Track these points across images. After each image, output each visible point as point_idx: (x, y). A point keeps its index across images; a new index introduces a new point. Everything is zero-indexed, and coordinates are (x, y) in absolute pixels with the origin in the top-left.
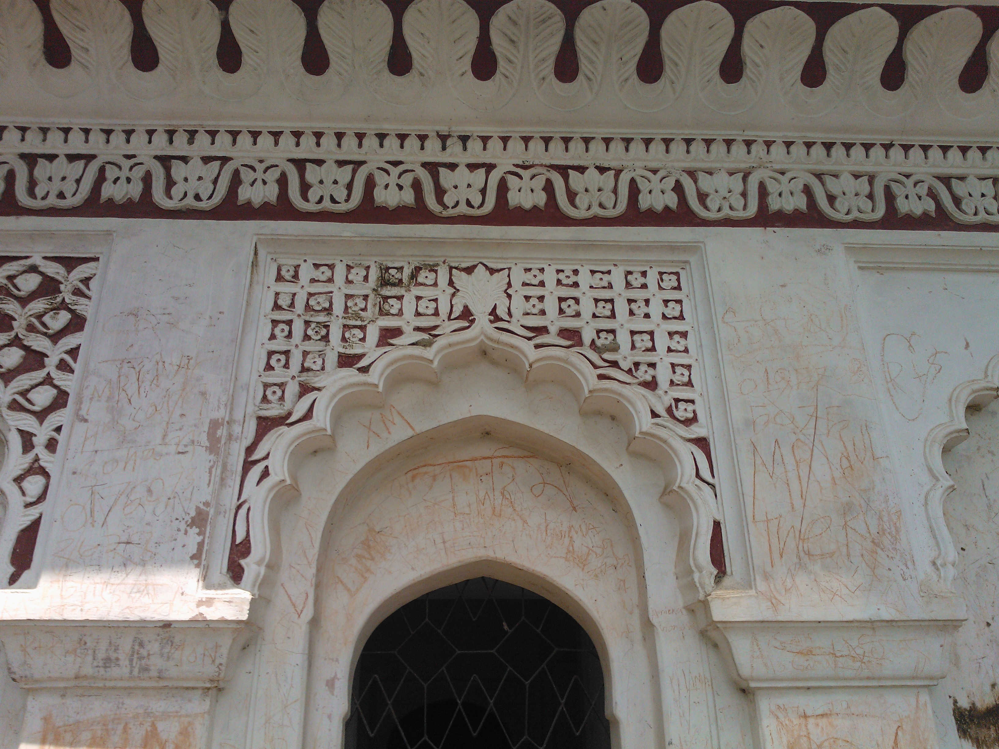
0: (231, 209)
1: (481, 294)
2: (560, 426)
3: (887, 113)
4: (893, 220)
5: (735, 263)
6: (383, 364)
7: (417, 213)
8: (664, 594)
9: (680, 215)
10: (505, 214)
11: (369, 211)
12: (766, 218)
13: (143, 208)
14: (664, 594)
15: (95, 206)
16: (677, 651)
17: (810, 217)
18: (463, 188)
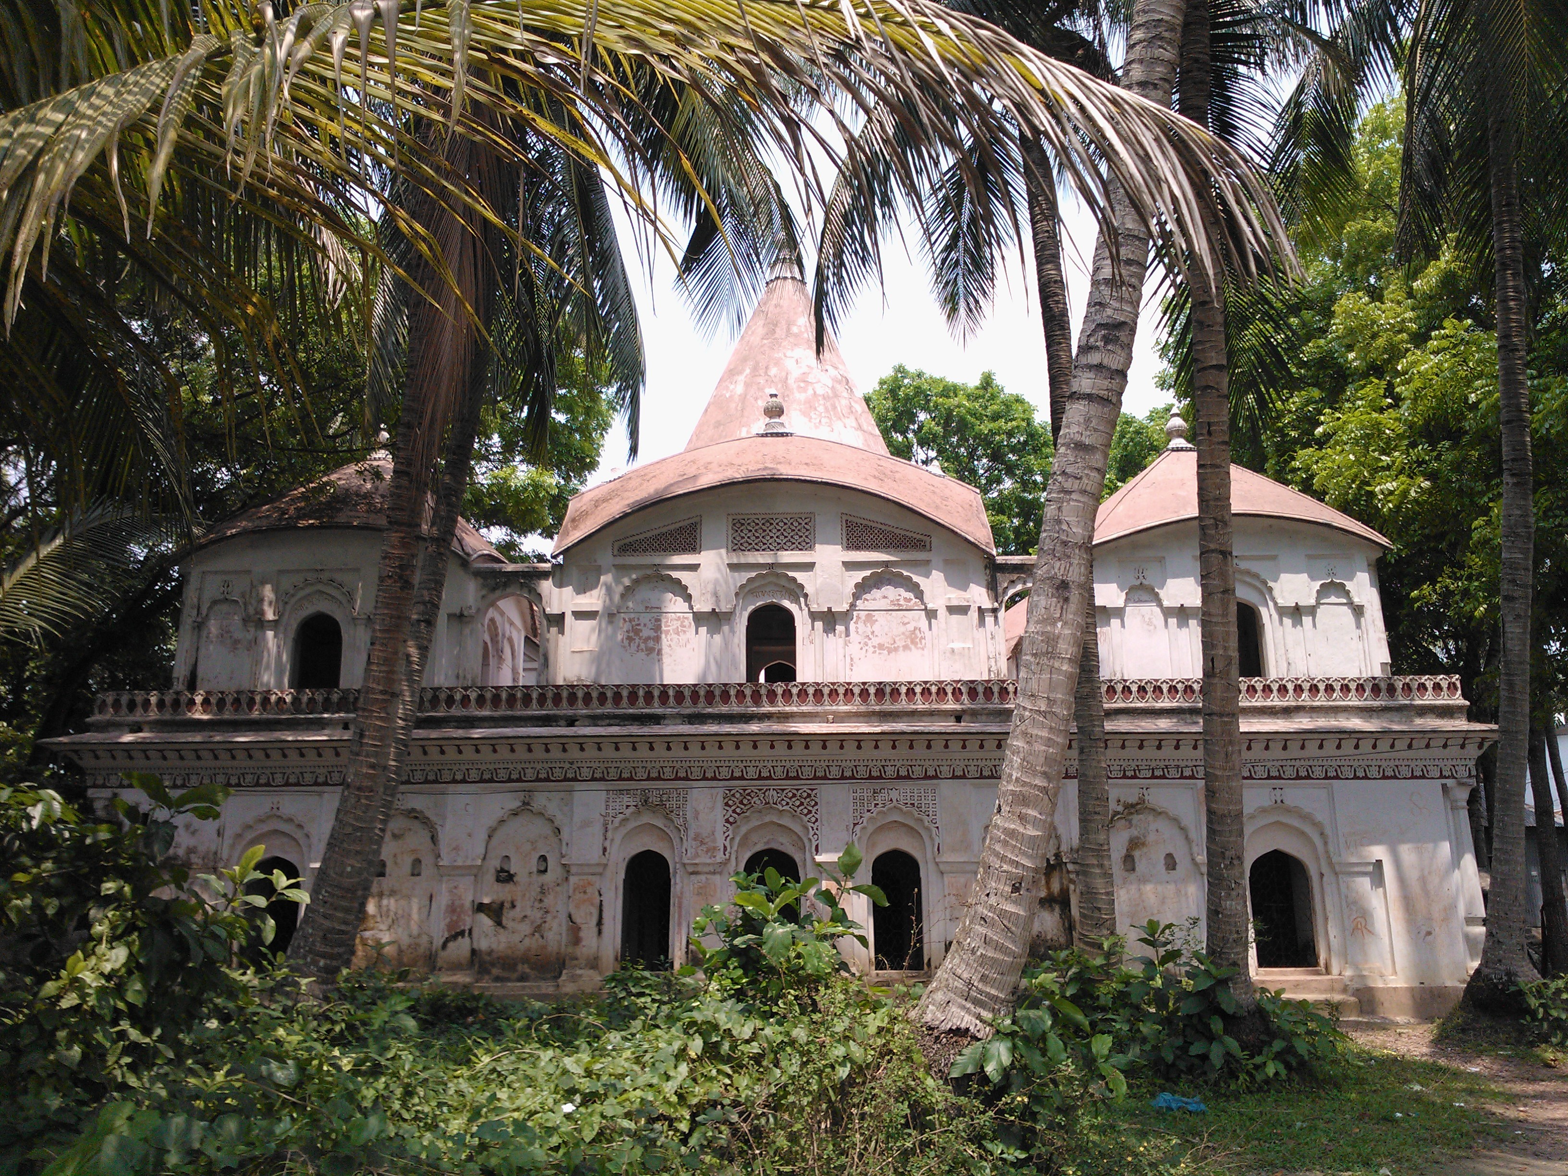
0: (843, 778)
1: (894, 795)
2: (912, 823)
3: (981, 754)
4: (982, 777)
5: (947, 788)
6: (875, 811)
7: (880, 777)
8: (929, 856)
9: (935, 777)
10: (899, 777)
11: (871, 777)
12: (954, 777)
13: (825, 778)
14: (929, 856)
15: (815, 778)
16: (931, 867)
17: (963, 777)
18: (890, 771)
